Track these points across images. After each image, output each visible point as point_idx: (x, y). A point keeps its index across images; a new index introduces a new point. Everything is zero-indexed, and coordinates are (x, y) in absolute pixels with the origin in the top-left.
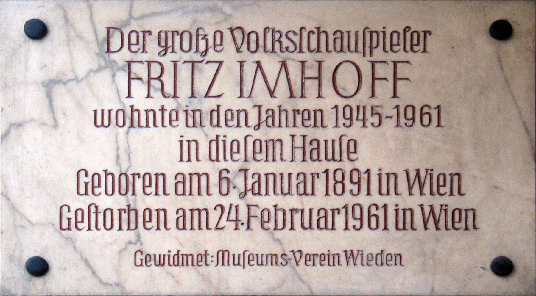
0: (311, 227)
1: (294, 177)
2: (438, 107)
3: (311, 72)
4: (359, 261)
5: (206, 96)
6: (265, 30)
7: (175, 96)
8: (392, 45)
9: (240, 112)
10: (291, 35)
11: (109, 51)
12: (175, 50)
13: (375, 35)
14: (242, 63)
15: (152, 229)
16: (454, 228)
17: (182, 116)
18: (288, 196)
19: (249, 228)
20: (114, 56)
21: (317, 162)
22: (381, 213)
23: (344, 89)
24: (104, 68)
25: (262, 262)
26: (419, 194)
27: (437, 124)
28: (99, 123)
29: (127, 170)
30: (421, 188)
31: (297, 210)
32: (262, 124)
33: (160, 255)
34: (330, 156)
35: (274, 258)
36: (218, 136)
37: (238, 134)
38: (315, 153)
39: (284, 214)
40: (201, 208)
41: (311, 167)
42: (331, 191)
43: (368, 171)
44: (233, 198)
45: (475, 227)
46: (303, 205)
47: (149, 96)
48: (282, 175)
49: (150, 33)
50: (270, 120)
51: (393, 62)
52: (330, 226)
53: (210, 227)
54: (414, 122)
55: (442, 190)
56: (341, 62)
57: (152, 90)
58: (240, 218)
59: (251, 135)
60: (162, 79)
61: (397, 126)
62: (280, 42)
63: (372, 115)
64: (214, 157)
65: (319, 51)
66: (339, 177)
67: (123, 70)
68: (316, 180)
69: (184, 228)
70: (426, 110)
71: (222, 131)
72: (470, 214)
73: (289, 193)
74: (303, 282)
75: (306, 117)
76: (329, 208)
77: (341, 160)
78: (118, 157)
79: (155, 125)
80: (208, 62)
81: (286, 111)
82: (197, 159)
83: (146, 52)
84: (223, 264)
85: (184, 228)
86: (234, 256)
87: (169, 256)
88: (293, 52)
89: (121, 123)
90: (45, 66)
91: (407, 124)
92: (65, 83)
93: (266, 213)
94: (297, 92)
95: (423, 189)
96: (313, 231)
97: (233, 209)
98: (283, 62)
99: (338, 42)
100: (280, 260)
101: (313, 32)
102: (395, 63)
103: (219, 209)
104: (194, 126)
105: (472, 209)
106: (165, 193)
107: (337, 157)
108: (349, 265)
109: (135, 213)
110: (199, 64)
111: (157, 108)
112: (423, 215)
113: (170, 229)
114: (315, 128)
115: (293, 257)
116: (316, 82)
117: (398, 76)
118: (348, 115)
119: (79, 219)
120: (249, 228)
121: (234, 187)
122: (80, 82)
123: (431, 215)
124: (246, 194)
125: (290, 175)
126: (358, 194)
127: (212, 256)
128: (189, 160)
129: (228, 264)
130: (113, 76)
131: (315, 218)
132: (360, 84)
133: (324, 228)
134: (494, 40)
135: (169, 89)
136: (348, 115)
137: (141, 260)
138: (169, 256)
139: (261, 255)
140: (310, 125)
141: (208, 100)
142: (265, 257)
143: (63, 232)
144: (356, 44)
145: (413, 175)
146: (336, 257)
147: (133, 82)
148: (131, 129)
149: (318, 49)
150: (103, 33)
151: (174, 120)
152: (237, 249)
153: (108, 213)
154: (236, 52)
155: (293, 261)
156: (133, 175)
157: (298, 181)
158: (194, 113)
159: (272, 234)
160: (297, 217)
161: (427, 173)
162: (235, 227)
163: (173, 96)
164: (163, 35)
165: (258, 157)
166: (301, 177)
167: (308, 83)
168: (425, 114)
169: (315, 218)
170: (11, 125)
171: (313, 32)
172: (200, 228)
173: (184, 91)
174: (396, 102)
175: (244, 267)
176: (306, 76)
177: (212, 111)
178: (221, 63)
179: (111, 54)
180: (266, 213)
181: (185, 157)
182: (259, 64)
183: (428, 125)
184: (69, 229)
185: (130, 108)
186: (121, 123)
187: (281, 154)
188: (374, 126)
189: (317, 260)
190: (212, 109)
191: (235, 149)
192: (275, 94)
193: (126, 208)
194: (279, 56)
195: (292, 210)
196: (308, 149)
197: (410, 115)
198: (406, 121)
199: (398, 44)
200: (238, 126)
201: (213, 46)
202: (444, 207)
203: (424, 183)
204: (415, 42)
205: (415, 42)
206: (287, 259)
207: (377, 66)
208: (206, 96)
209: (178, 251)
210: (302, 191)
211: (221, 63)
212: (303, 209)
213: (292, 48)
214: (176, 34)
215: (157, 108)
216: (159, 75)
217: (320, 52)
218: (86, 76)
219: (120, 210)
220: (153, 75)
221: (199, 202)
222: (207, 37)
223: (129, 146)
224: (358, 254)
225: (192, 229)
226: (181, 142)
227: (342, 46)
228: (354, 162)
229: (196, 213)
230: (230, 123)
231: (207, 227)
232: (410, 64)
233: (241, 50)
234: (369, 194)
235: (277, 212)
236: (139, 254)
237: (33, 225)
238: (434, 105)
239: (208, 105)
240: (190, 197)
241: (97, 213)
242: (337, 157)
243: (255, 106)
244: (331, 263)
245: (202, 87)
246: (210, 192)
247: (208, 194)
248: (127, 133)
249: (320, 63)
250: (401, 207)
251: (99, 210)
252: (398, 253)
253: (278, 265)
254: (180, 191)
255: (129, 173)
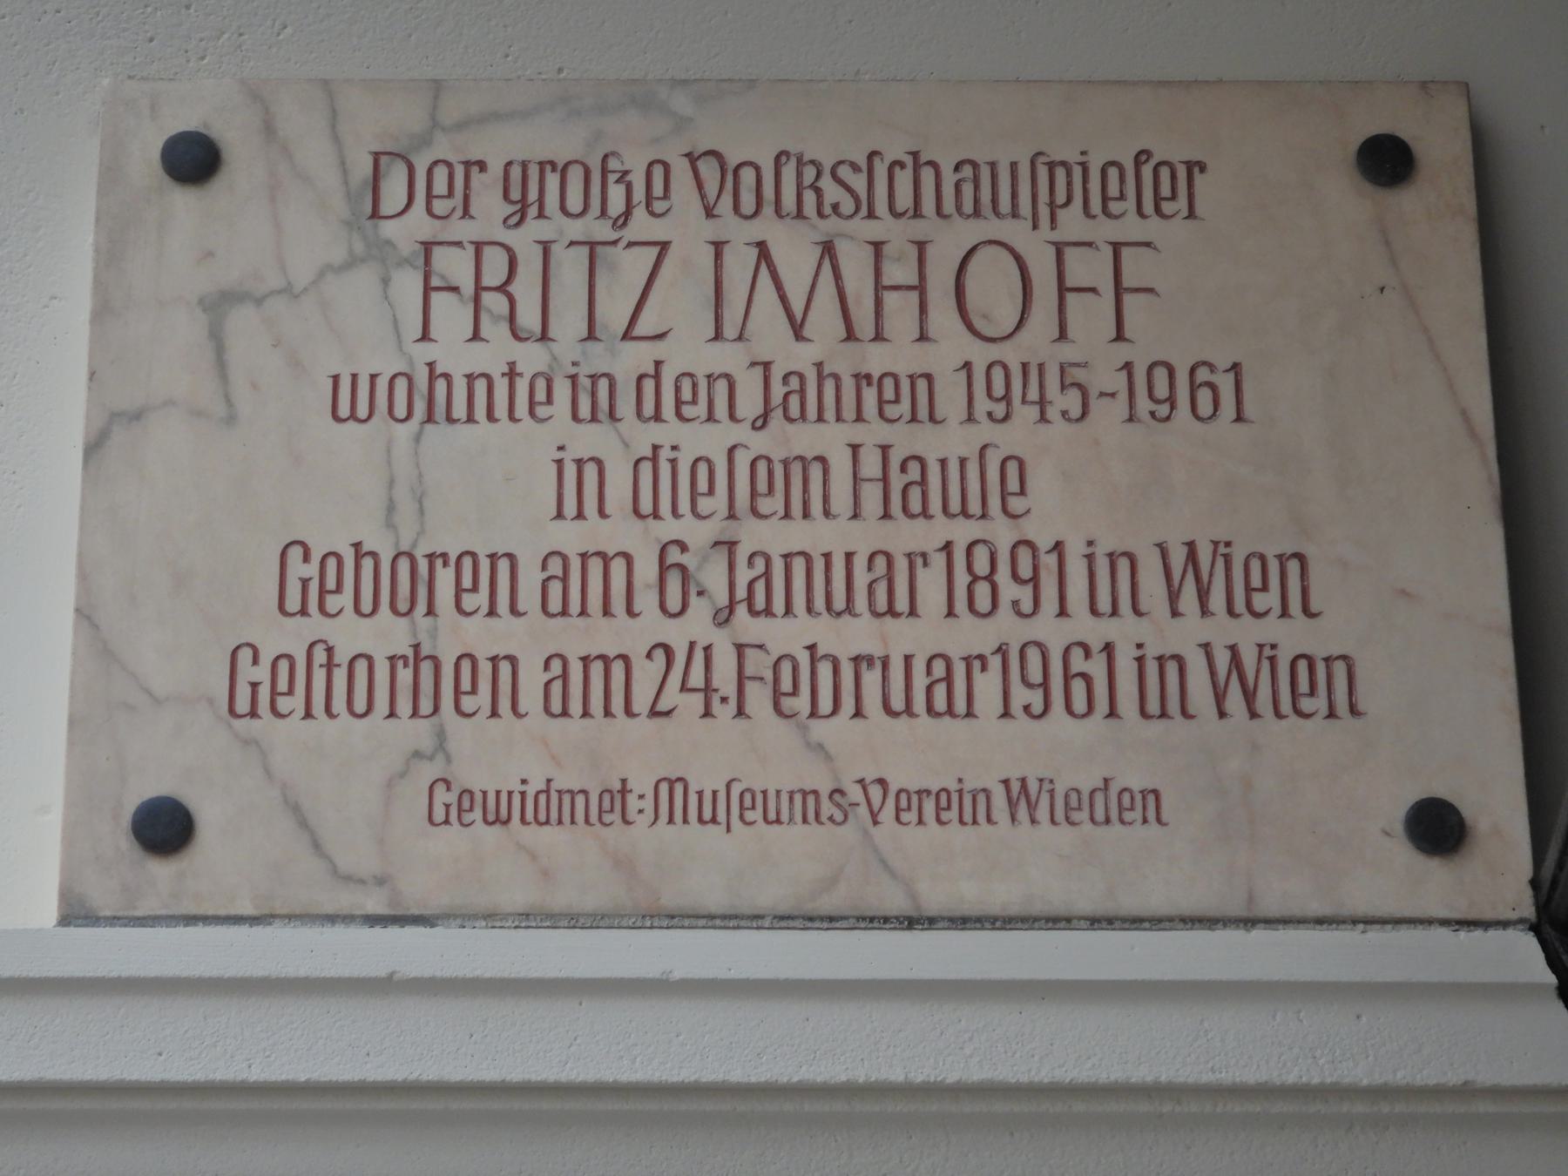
0: (909, 710)
1: (860, 563)
2: (1235, 367)
3: (899, 272)
4: (1043, 813)
5: (627, 336)
6: (777, 158)
7: (544, 337)
8: (1105, 199)
9: (714, 380)
10: (844, 172)
11: (375, 214)
12: (548, 211)
13: (1060, 174)
14: (718, 247)
15: (477, 716)
16: (1299, 712)
17: (562, 391)
18: (846, 618)
19: (740, 712)
20: (389, 229)
21: (921, 521)
22: (1097, 668)
23: (985, 317)
24: (363, 260)
25: (778, 813)
26: (1200, 613)
27: (1234, 416)
28: (344, 411)
29: (414, 545)
30: (1203, 595)
31: (870, 660)
32: (773, 414)
33: (498, 793)
34: (955, 505)
35: (811, 800)
36: (656, 448)
37: (709, 441)
38: (915, 494)
39: (836, 671)
40: (612, 653)
41: (907, 536)
42: (961, 605)
43: (1058, 547)
44: (697, 625)
45: (1354, 711)
46: (886, 644)
47: (476, 336)
48: (827, 556)
49: (482, 166)
50: (794, 401)
51: (1111, 243)
52: (960, 705)
53: (636, 709)
54: (1172, 408)
55: (1260, 601)
56: (976, 243)
57: (485, 320)
58: (715, 683)
59: (745, 443)
60: (511, 289)
61: (1131, 419)
62: (818, 192)
63: (1063, 387)
64: (646, 505)
65: (917, 213)
66: (982, 565)
67: (411, 265)
68: (921, 572)
69: (565, 713)
70: (1203, 375)
71: (668, 432)
72: (1340, 669)
73: (849, 609)
74: (892, 874)
75: (889, 394)
76: (955, 654)
77: (984, 516)
78: (391, 508)
79: (491, 417)
80: (631, 244)
81: (837, 378)
82: (602, 513)
83: (472, 217)
84: (671, 821)
85: (565, 713)
86: (700, 794)
87: (523, 794)
88: (851, 216)
89: (401, 411)
90: (210, 254)
91: (1156, 414)
92: (259, 302)
93: (786, 669)
94: (865, 326)
95: (1207, 601)
96: (914, 721)
97: (699, 656)
98: (826, 242)
99: (968, 189)
100: (827, 808)
101: (902, 165)
102: (1116, 247)
103: (660, 655)
104: (594, 419)
105: (1344, 657)
106: (514, 611)
107: (975, 507)
108: (1016, 823)
109: (433, 666)
110: (609, 249)
111: (497, 370)
112: (1213, 673)
113: (527, 714)
114: (914, 425)
115: (860, 798)
116: (914, 297)
117: (1127, 282)
118: (999, 390)
119: (283, 686)
120: (740, 712)
121: (700, 593)
122: (296, 297)
123: (1234, 676)
124: (731, 612)
125: (849, 556)
126: (1034, 613)
127: (641, 797)
128: (580, 515)
129: (685, 821)
130: (386, 281)
131: (920, 681)
132: (1028, 304)
133: (945, 713)
134: (1368, 187)
135: (529, 317)
136: (999, 390)
137: (447, 806)
138: (523, 794)
139: (774, 792)
140: (901, 417)
141: (630, 346)
142: (785, 798)
143: (237, 723)
144: (1014, 195)
145: (1178, 558)
146: (981, 798)
147: (436, 297)
148: (429, 427)
149: (916, 210)
150: (362, 167)
151: (541, 403)
152: (706, 779)
153: (361, 668)
154: (704, 217)
155: (863, 810)
156: (431, 557)
157: (872, 576)
158: (594, 384)
159: (804, 729)
160: (872, 679)
161: (1215, 552)
162: (702, 710)
163: (540, 336)
164: (516, 172)
165: (765, 505)
166: (880, 562)
167: (890, 299)
168: (1200, 385)
169: (920, 681)
170: (114, 416)
171: (902, 165)
172: (608, 713)
173: (569, 322)
174: (1123, 352)
175: (728, 830)
176: (886, 281)
177: (641, 378)
178: (664, 246)
179: (383, 223)
180: (786, 669)
181: (570, 507)
182: (762, 246)
183: (1210, 418)
184: (253, 714)
185: (426, 369)
186: (401, 411)
187: (826, 499)
188: (1069, 420)
189: (929, 807)
190: (642, 371)
191: (703, 486)
192: (807, 331)
193: (410, 653)
194: (814, 227)
195: (856, 660)
196: (897, 482)
197: (1162, 390)
198: (1153, 407)
199: (1122, 197)
200: (710, 418)
201: (644, 201)
202: (1267, 652)
203: (1210, 582)
204: (1165, 190)
205: (1165, 190)
206: (846, 806)
207: (1071, 254)
208: (627, 336)
209: (549, 781)
210: (882, 603)
211: (664, 246)
212: (887, 656)
213: (847, 206)
214: (548, 168)
215: (497, 370)
216: (504, 278)
217: (922, 216)
218: (314, 282)
219: (392, 659)
220: (487, 281)
221: (607, 636)
222: (628, 178)
223: (420, 475)
224: (1040, 792)
225: (586, 714)
226: (560, 462)
227: (976, 201)
228: (1020, 520)
229: (597, 668)
230: (687, 411)
231: (629, 712)
232: (1155, 248)
233: (715, 212)
234: (1063, 612)
235: (816, 663)
236: (440, 789)
237: (157, 701)
238: (1223, 363)
239: (630, 360)
240: (581, 622)
241: (330, 666)
242: (975, 507)
243: (753, 364)
244: (968, 817)
245: (614, 312)
246: (637, 608)
247: (630, 612)
248: (418, 438)
249: (921, 246)
250: (1151, 652)
251: (336, 660)
252: (1151, 787)
253: (822, 824)
254: (555, 605)
255: (419, 553)
